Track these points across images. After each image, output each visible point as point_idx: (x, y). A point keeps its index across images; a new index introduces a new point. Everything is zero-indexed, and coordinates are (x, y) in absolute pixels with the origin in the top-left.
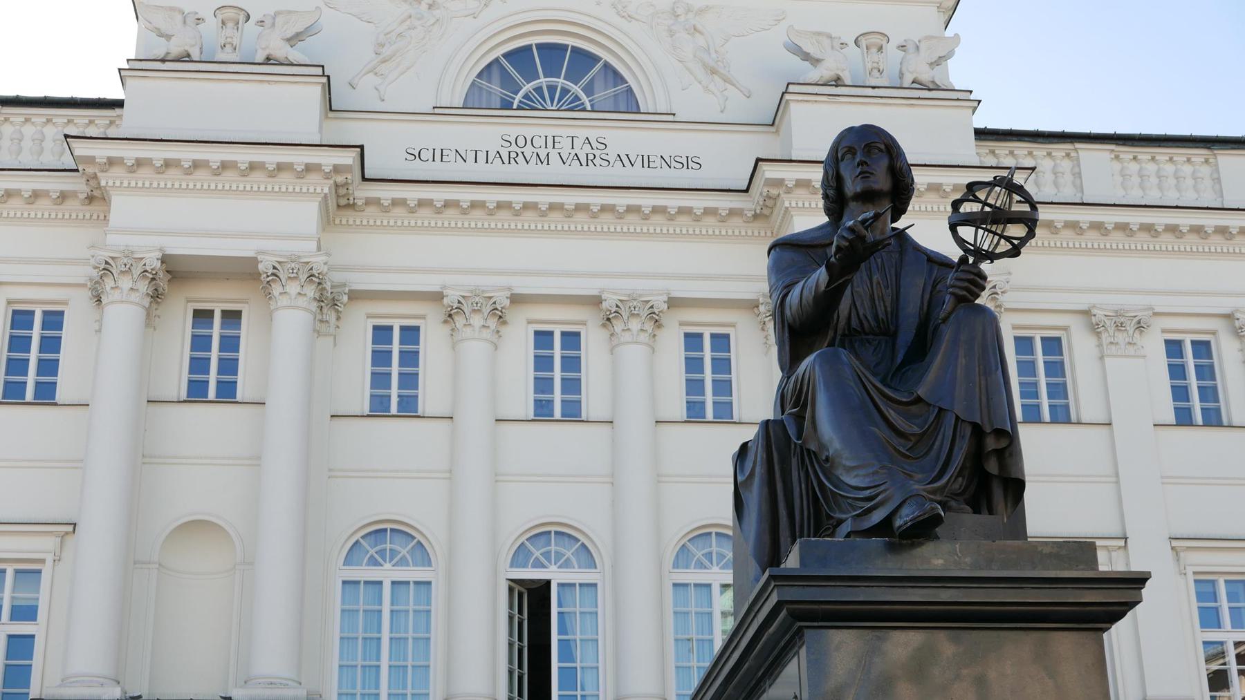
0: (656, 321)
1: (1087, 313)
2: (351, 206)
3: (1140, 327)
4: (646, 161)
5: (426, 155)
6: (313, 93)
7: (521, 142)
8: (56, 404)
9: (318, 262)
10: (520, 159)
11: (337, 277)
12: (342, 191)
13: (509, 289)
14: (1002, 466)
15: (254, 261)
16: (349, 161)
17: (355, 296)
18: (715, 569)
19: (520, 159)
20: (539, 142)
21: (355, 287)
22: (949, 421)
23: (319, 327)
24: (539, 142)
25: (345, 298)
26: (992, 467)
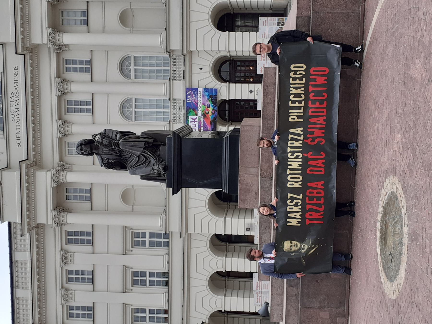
0: (64, 80)
4: (16, 81)
5: (19, 142)
6: (5, 173)
7: (13, 116)
8: (92, 232)
9: (54, 171)
10: (18, 116)
11: (55, 165)
12: (32, 165)
13: (56, 121)
14: (150, 143)
15: (53, 188)
16: (24, 165)
17: (61, 160)
18: (131, 67)
19: (18, 116)
20: (12, 111)
21: (58, 160)
22: (142, 153)
24: (12, 111)
25: (61, 163)
26: (151, 145)
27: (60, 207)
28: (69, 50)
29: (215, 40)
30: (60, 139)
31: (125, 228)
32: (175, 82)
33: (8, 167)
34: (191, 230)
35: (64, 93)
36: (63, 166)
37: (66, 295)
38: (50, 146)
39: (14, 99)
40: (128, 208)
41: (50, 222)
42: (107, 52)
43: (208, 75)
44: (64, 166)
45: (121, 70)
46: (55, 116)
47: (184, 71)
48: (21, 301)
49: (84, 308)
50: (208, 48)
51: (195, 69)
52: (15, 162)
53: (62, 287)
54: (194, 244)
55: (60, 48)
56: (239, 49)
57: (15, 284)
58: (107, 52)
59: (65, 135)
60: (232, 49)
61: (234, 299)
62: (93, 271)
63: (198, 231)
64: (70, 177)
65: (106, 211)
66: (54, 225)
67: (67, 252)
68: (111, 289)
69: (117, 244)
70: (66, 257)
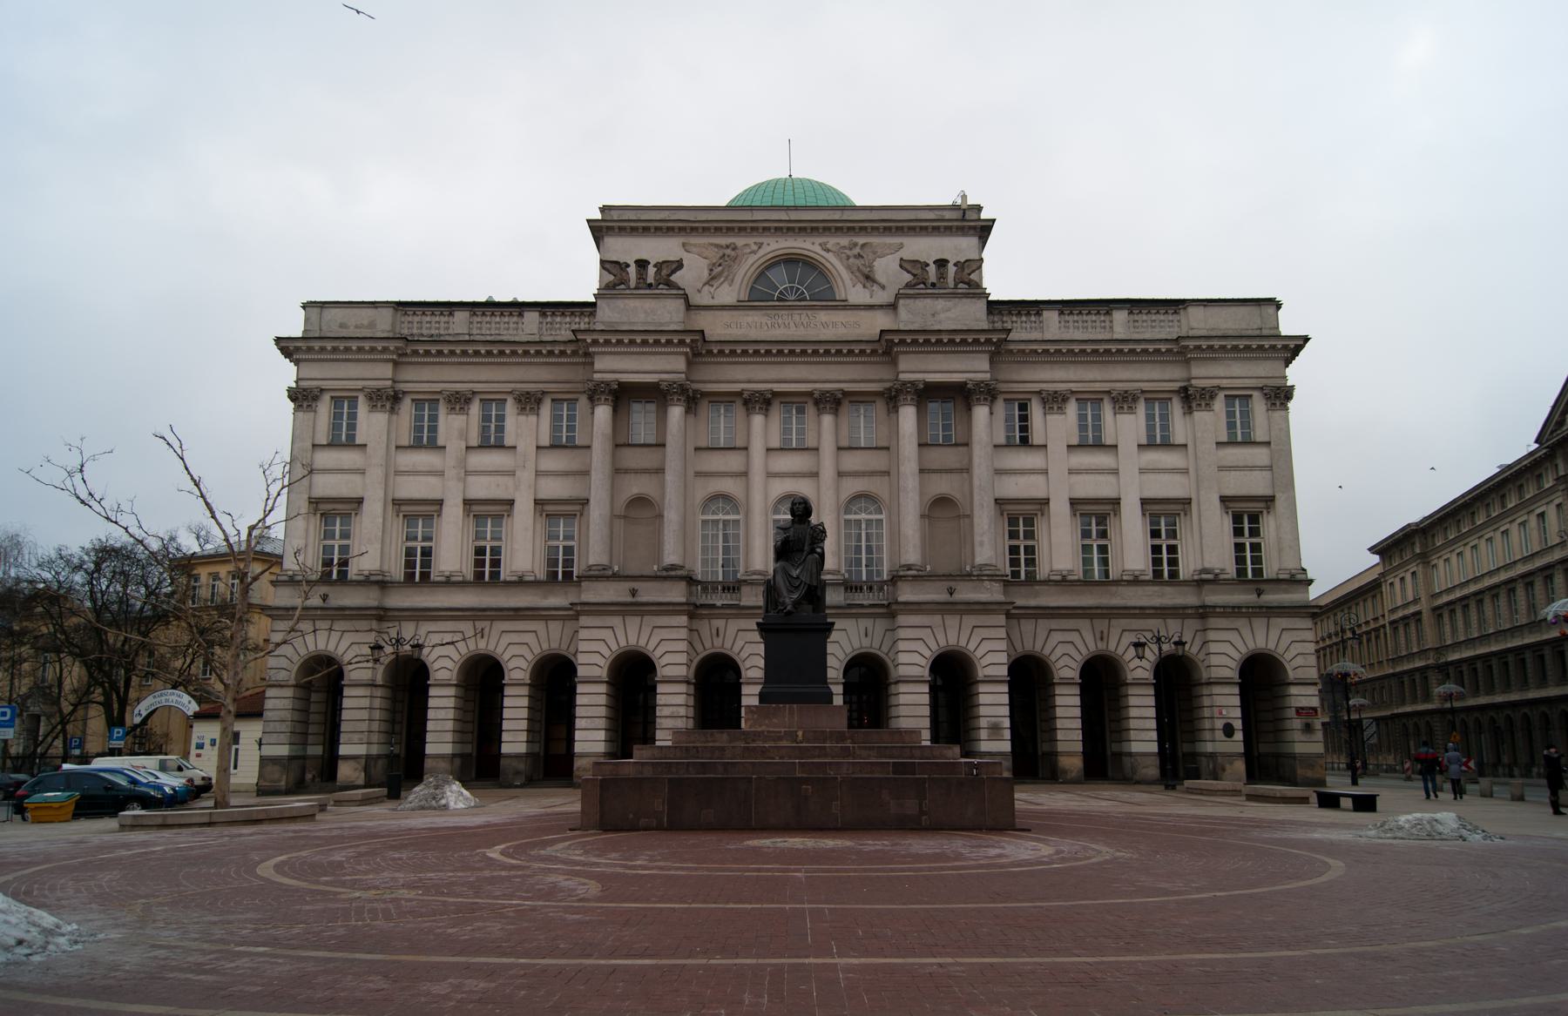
1: (1039, 393)
2: (700, 355)
3: (1065, 400)
4: (834, 324)
6: (680, 303)
11: (695, 386)
17: (705, 394)
23: (687, 412)
27: (622, 395)
28: (889, 412)
29: (917, 659)
30: (739, 394)
31: (585, 502)
32: (842, 589)
33: (689, 306)
34: (584, 620)
35: (817, 403)
36: (694, 398)
37: (459, 401)
38: (729, 377)
39: (805, 319)
40: (620, 510)
41: (597, 376)
42: (888, 473)
43: (856, 645)
44: (693, 400)
45: (858, 497)
46: (777, 387)
47: (862, 606)
48: (443, 319)
49: (433, 429)
50: (902, 646)
51: (865, 623)
52: (703, 321)
53: (474, 393)
54: (555, 626)
55: (891, 398)
56: (903, 699)
57: (479, 311)
58: (888, 473)
59: (746, 403)
60: (903, 688)
61: (451, 702)
62: (503, 447)
63: (583, 634)
64: (676, 412)
65: (618, 471)
66: (591, 385)
67: (539, 402)
68: (470, 479)
69: (554, 489)
70: (529, 402)
